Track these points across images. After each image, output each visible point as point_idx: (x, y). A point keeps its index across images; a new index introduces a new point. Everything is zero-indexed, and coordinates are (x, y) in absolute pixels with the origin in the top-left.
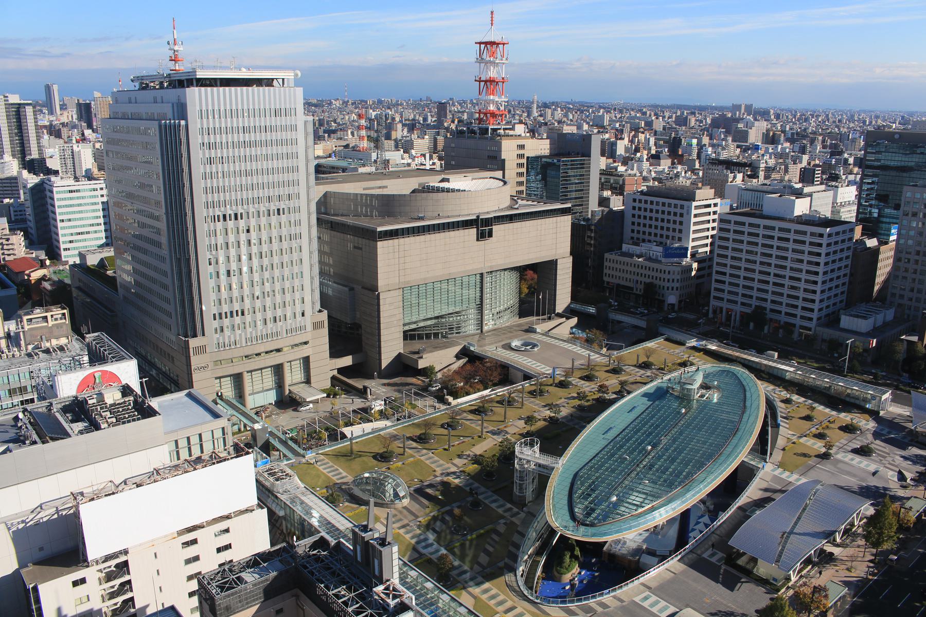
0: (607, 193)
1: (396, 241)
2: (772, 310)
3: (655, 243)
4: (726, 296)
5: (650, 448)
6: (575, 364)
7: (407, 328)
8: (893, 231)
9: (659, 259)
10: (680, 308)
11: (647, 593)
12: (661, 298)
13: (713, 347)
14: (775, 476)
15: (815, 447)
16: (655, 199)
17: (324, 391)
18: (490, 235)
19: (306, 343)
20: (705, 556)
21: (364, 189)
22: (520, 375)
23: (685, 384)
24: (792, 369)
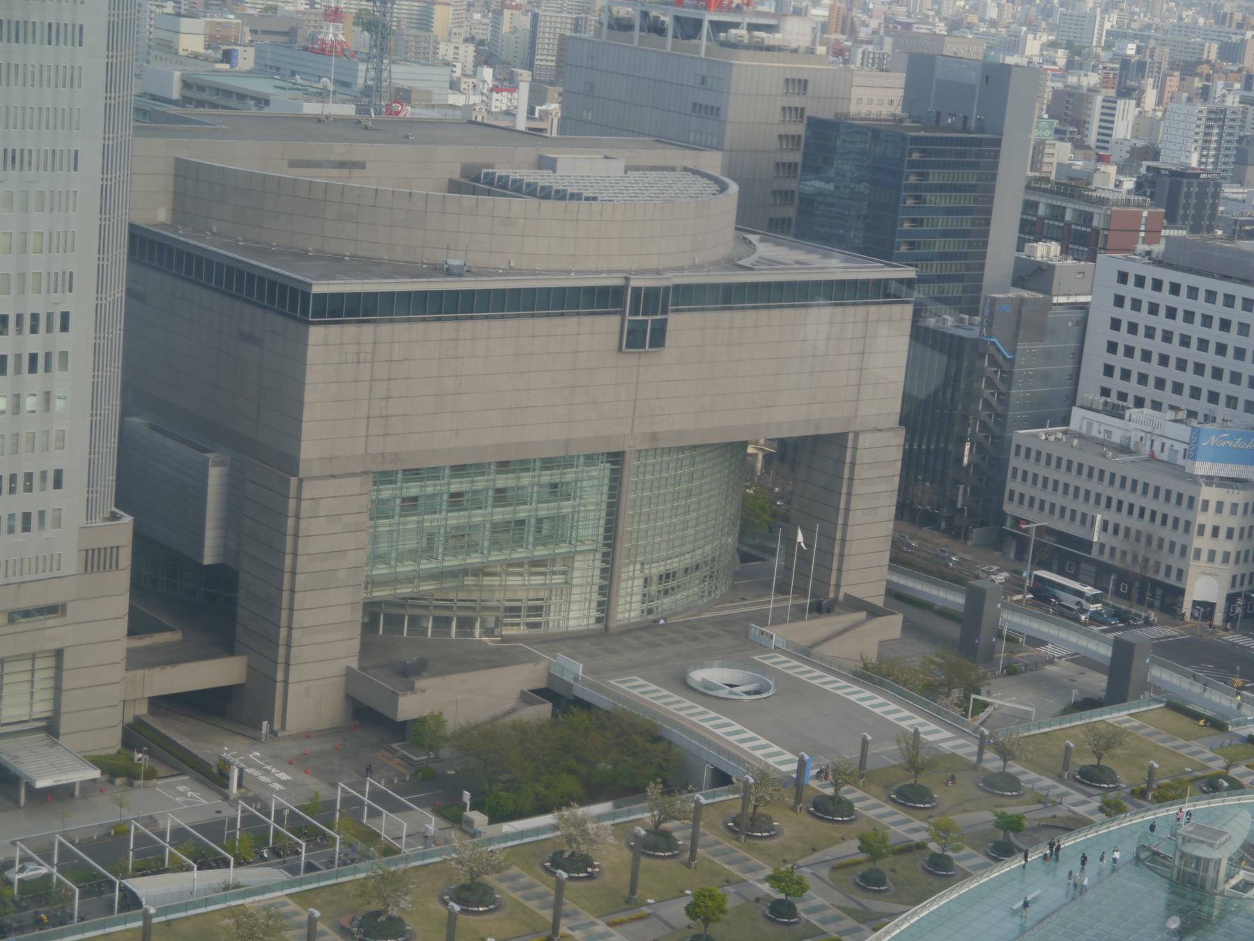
0: (1046, 251)
1: (368, 329)
3: (1170, 415)
6: (872, 750)
7: (380, 593)
9: (1180, 461)
10: (1229, 618)
12: (1172, 581)
16: (1185, 280)
17: (96, 762)
18: (658, 338)
19: (54, 610)
21: (294, 164)
22: (706, 776)
23: (1186, 840)
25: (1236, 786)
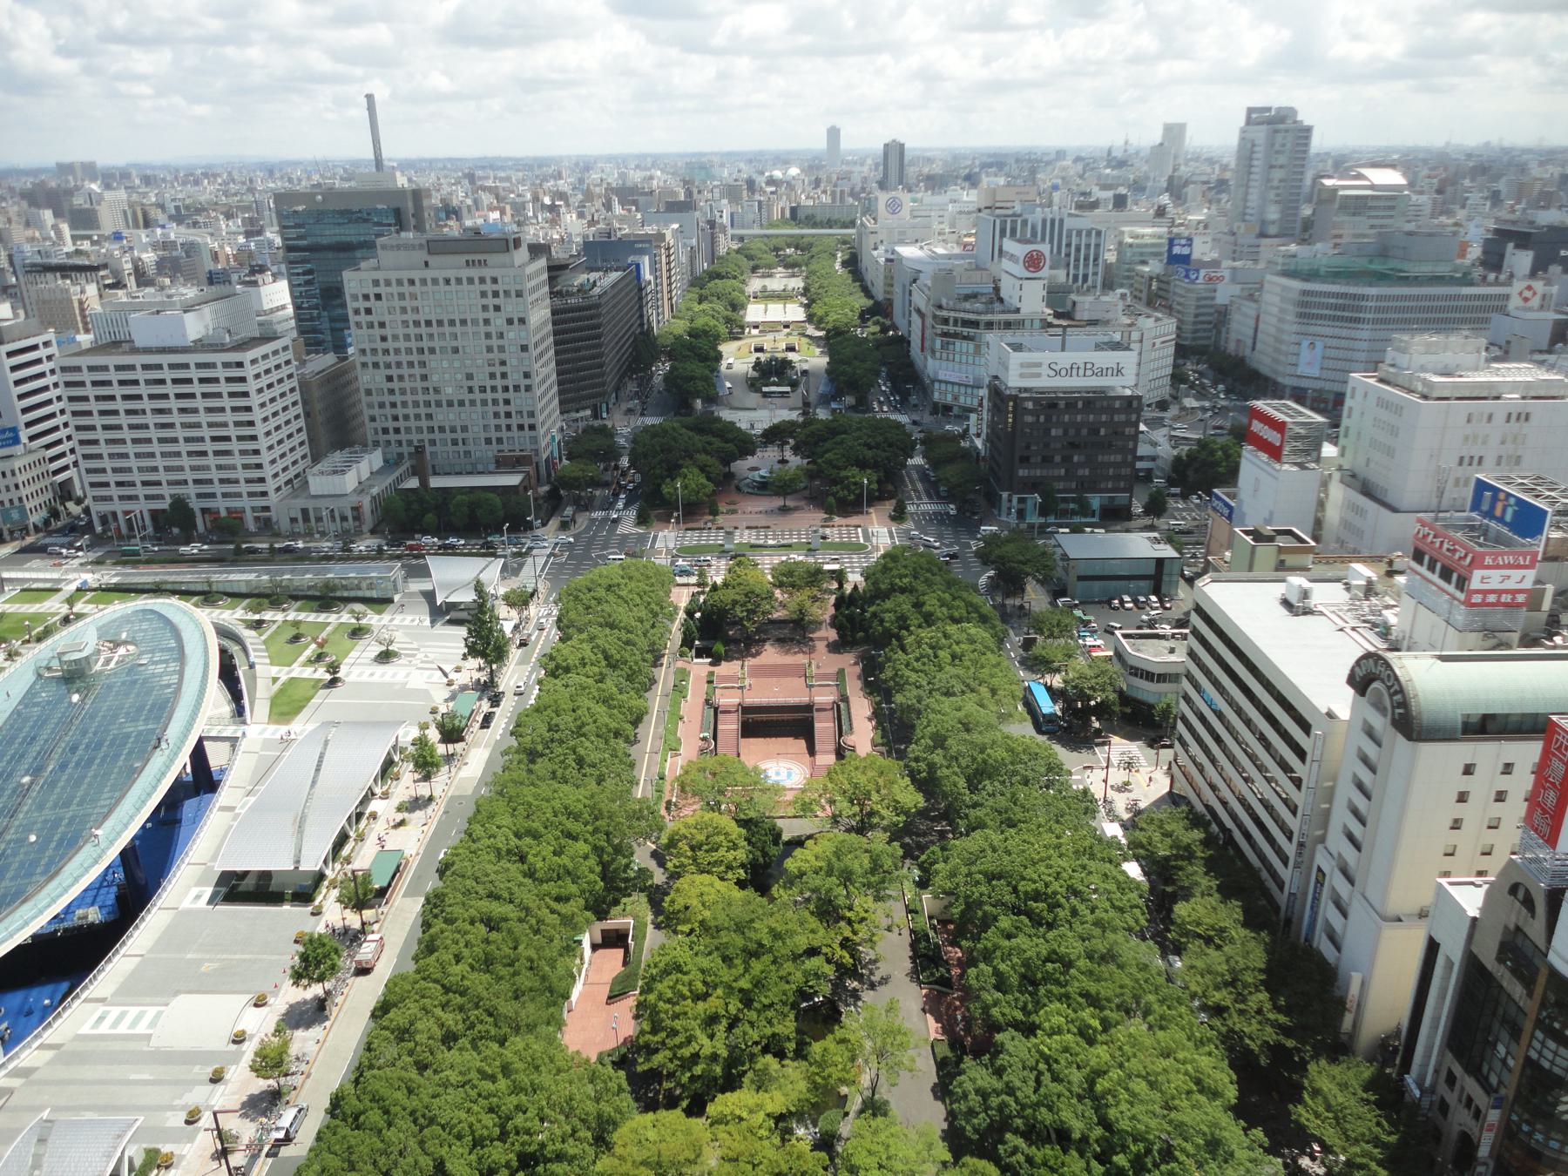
2: (199, 496)
4: (114, 491)
5: (26, 779)
8: (349, 340)
11: (101, 1009)
13: (111, 576)
14: (265, 740)
15: (317, 676)
20: (186, 904)
24: (252, 577)
25: (79, 616)
